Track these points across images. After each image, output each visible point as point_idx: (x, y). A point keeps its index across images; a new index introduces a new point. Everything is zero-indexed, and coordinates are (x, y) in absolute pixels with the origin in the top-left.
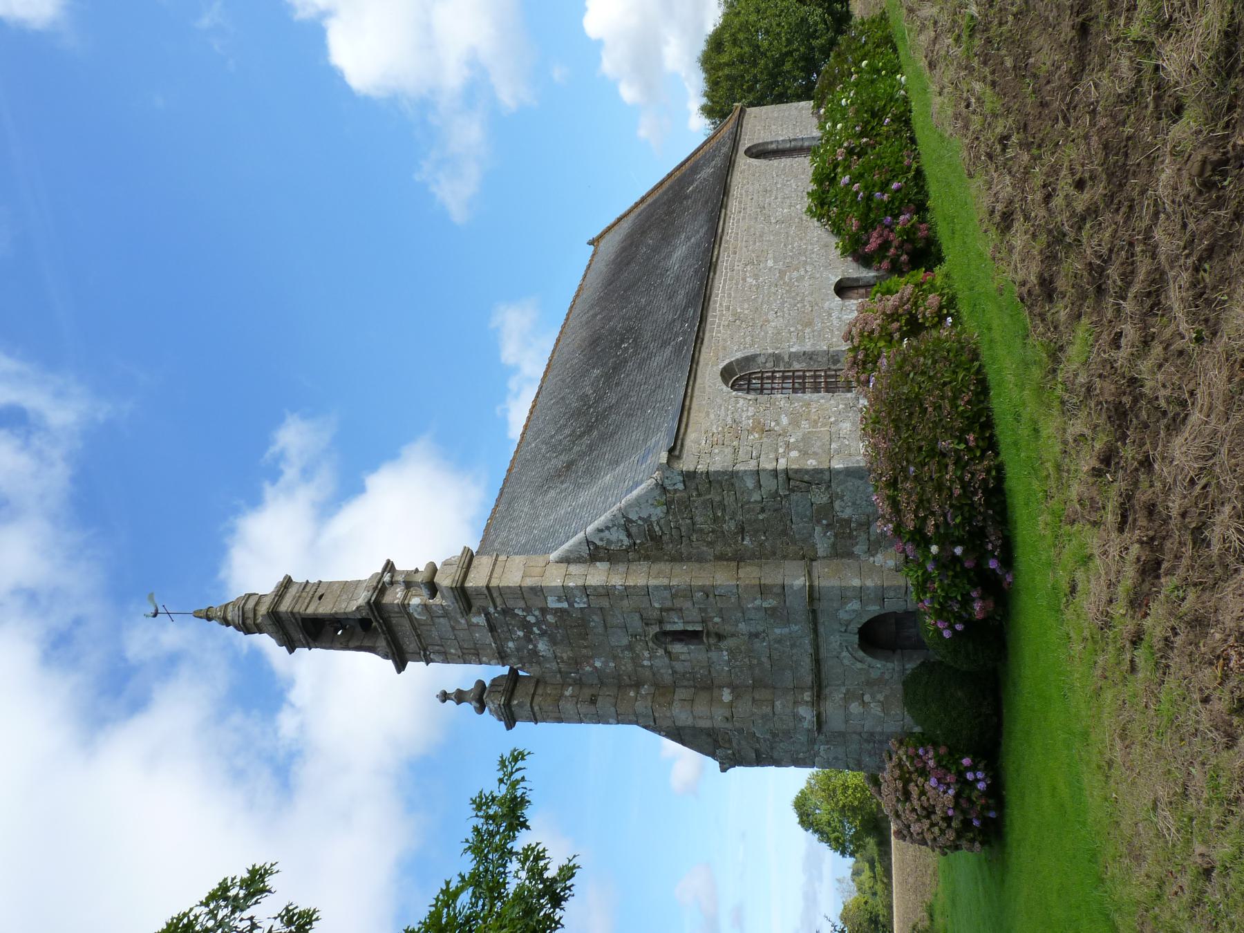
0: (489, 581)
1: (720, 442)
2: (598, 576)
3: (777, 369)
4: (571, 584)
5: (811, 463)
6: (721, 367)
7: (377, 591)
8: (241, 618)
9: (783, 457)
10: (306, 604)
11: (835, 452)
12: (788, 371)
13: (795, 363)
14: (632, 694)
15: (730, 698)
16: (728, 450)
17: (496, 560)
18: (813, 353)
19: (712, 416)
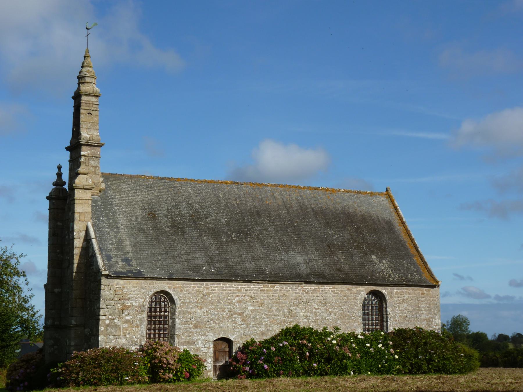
0: (77, 199)
1: (117, 293)
2: (78, 243)
3: (170, 313)
4: (75, 233)
5: (102, 328)
6: (167, 290)
7: (86, 143)
8: (81, 76)
9: (106, 318)
10: (85, 108)
11: (107, 337)
12: (169, 318)
13: (172, 320)
14: (58, 251)
15: (56, 292)
16: (112, 297)
17: (88, 200)
18: (175, 328)
19: (134, 289)
